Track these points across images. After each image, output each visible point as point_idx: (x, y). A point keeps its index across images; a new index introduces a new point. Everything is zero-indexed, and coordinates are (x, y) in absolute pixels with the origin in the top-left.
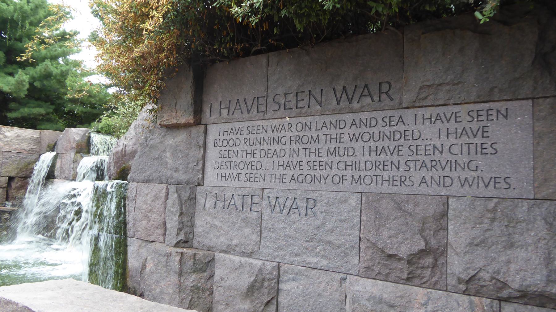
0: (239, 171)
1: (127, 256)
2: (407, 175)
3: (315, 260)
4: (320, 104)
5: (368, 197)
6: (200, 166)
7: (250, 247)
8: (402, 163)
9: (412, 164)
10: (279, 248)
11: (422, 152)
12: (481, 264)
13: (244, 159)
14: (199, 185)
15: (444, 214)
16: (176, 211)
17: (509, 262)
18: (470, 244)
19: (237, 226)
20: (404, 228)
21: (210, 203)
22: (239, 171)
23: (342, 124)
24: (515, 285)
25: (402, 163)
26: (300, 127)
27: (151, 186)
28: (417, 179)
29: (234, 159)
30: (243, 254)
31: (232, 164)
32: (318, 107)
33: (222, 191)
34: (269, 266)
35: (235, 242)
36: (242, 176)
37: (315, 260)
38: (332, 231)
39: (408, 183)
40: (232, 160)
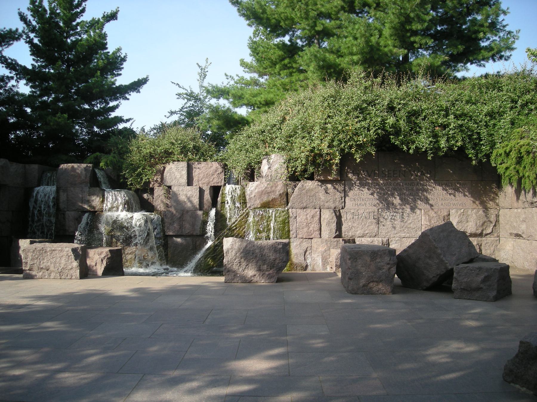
0: (365, 202)
1: (3, 304)
2: (437, 202)
3: (404, 235)
4: (404, 176)
5: (424, 210)
6: (343, 200)
7: (375, 233)
8: (435, 199)
9: (438, 199)
10: (388, 232)
11: (441, 195)
12: (460, 228)
13: (368, 197)
14: (342, 209)
15: (449, 215)
16: (334, 221)
17: (467, 226)
18: (458, 222)
19: (367, 225)
20: (439, 220)
21: (349, 216)
22: (365, 202)
23: (413, 184)
24: (469, 232)
25: (435, 199)
26: (395, 184)
27: (309, 211)
28: (440, 204)
29: (362, 197)
30: (370, 237)
31: (361, 199)
32: (404, 177)
33: (357, 211)
34: (385, 240)
35: (366, 232)
36: (368, 204)
37: (404, 235)
38: (411, 223)
39: (437, 205)
40: (361, 197)
